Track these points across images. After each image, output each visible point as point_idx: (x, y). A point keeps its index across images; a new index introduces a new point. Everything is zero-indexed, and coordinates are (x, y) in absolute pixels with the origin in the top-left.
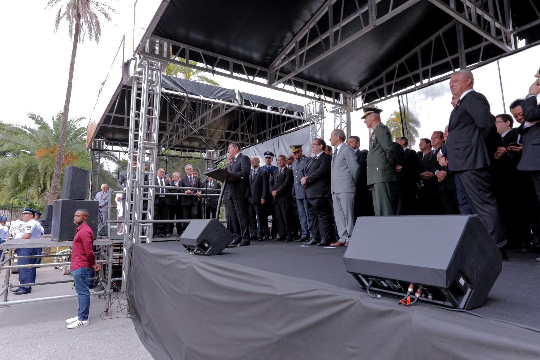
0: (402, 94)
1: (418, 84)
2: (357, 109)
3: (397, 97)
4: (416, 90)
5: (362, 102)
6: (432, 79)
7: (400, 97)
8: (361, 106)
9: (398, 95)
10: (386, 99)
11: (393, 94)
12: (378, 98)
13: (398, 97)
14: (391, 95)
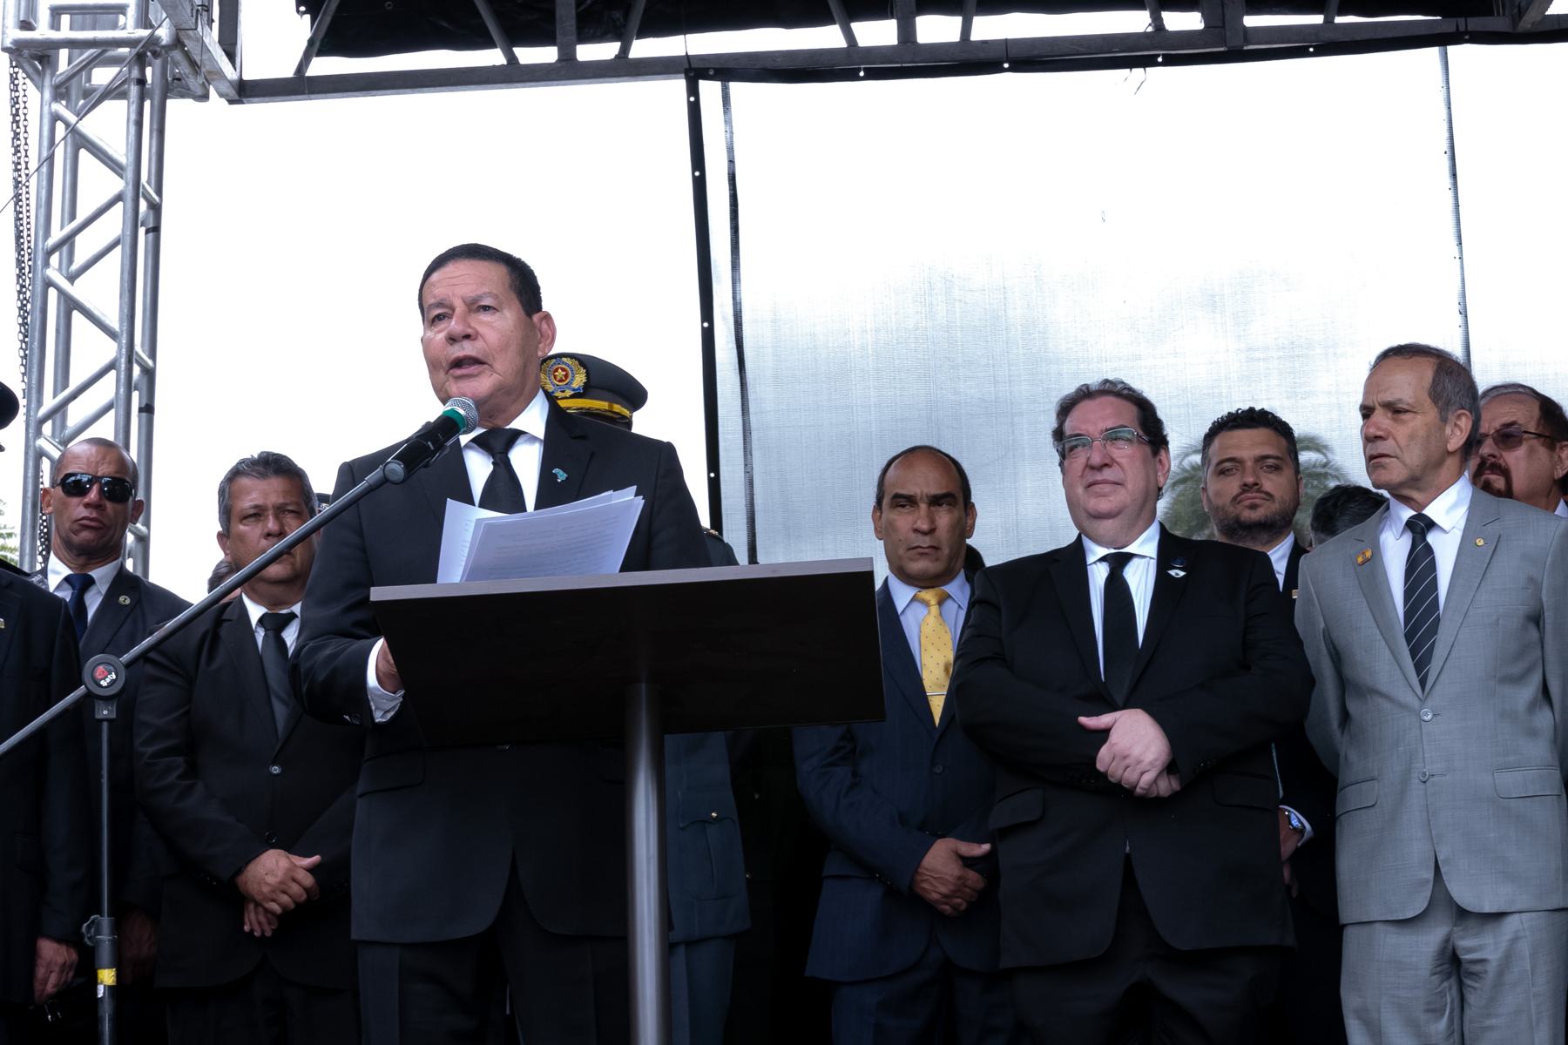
0: (729, 70)
1: (877, 33)
2: (245, 91)
3: (679, 85)
4: (850, 75)
5: (301, 28)
6: (991, 28)
7: (710, 90)
8: (288, 72)
9: (695, 71)
10: (568, 71)
11: (643, 48)
12: (477, 39)
13: (693, 90)
14: (625, 50)
